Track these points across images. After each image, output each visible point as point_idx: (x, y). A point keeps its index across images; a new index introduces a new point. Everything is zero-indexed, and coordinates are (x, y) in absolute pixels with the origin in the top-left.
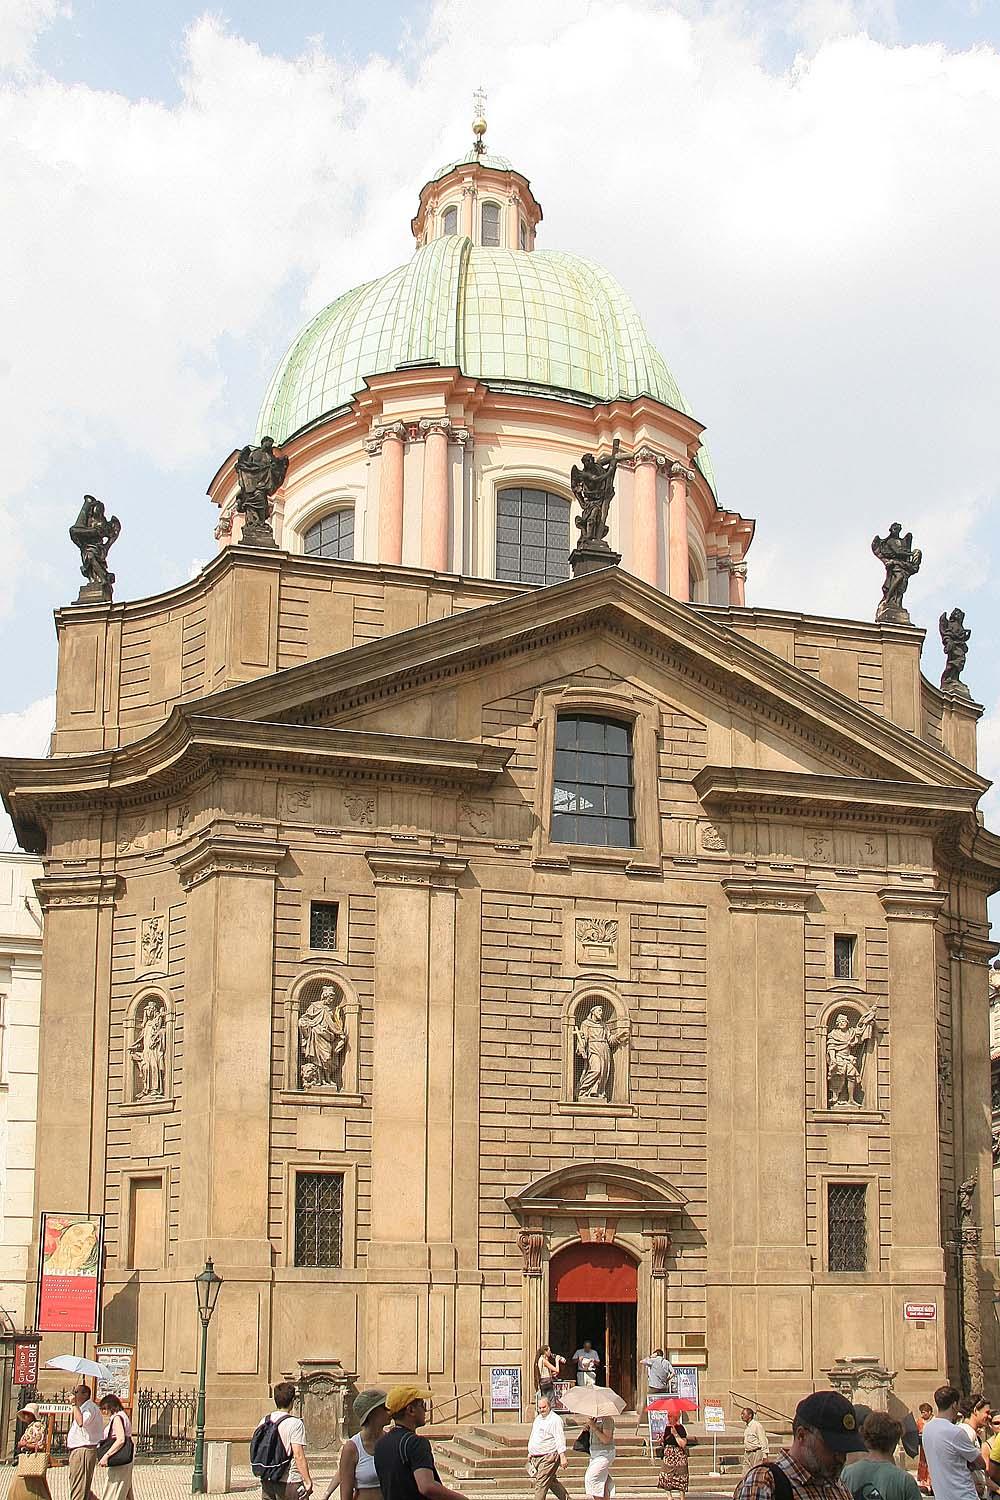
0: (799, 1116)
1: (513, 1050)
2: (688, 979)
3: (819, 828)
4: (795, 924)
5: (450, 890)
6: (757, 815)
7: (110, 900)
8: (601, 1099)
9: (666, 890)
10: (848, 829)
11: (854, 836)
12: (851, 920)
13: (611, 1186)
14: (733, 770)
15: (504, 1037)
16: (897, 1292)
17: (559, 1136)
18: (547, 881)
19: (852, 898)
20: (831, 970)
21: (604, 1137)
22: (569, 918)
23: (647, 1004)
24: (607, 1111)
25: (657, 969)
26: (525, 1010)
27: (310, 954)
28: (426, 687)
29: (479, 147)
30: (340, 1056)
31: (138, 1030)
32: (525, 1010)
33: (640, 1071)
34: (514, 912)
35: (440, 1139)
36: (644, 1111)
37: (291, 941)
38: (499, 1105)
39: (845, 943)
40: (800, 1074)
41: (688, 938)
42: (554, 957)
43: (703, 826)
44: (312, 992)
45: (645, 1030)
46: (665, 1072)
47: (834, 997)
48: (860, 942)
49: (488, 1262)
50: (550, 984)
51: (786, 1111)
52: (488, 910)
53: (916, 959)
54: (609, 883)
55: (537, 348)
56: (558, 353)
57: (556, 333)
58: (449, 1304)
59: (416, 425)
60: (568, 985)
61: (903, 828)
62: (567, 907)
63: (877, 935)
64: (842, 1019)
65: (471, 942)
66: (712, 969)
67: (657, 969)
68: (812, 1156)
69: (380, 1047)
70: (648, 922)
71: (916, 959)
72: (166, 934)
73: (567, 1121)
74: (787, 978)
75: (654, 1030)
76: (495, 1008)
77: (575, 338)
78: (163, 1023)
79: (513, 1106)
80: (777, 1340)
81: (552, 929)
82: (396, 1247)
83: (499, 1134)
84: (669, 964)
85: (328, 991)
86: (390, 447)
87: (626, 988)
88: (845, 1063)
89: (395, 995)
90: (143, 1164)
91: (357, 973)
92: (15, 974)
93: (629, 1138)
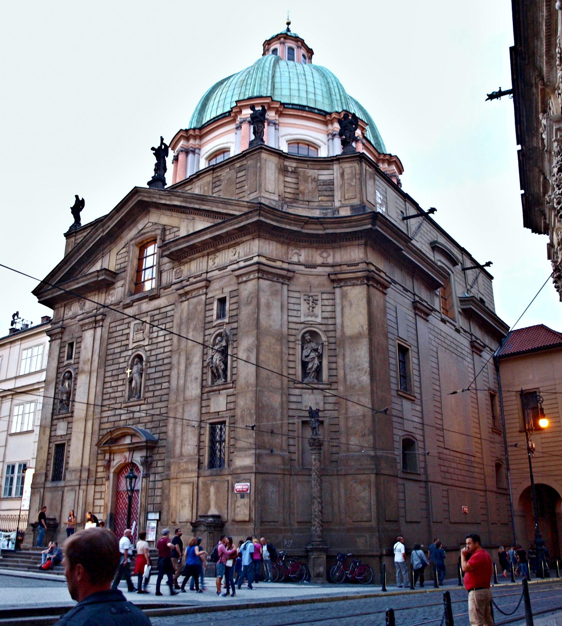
0: (199, 391)
1: (113, 384)
3: (214, 253)
4: (202, 299)
5: (100, 326)
6: (189, 257)
8: (135, 399)
10: (224, 249)
11: (227, 251)
16: (233, 477)
17: (123, 417)
19: (227, 279)
20: (215, 317)
22: (132, 326)
24: (137, 403)
25: (157, 337)
26: (117, 366)
27: (65, 363)
29: (288, 30)
32: (117, 366)
33: (149, 383)
34: (118, 328)
35: (90, 424)
36: (150, 400)
39: (222, 301)
40: (200, 371)
41: (169, 319)
43: (175, 270)
47: (216, 328)
49: (99, 475)
51: (194, 390)
52: (111, 330)
53: (249, 299)
58: (85, 493)
61: (244, 239)
62: (133, 321)
63: (235, 293)
65: (105, 344)
67: (157, 337)
68: (204, 410)
70: (156, 317)
71: (249, 299)
74: (197, 326)
80: (182, 506)
82: (74, 471)
89: (83, 372)
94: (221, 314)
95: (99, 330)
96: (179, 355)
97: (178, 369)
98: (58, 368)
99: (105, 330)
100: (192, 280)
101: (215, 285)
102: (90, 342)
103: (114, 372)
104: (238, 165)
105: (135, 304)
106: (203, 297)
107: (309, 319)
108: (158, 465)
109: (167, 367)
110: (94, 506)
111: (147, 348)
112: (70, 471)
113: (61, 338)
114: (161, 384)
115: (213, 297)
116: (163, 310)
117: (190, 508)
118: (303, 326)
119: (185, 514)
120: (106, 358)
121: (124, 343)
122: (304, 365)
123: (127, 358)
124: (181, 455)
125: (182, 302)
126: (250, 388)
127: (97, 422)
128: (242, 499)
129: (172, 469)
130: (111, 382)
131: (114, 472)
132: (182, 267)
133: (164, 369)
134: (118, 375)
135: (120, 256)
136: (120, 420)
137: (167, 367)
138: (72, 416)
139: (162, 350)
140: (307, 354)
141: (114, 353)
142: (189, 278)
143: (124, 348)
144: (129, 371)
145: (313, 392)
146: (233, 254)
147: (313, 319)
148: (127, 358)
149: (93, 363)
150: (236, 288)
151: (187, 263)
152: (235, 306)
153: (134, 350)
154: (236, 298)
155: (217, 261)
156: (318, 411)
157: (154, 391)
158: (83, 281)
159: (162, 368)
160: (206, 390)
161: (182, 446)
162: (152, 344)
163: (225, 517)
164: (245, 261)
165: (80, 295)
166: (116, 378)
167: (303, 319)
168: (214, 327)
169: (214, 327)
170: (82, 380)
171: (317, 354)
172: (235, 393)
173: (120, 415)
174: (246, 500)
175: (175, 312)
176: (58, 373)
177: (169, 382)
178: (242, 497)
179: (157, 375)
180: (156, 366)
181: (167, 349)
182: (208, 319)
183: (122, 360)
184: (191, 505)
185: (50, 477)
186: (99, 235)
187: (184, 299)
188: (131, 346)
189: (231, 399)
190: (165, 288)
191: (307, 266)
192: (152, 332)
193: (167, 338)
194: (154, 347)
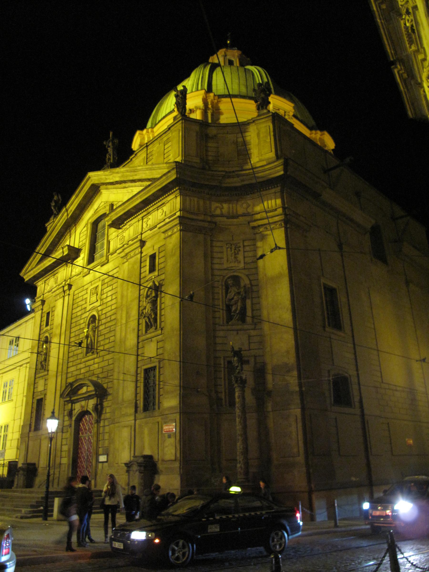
17: (83, 371)
25: (107, 297)
27: (44, 330)
28: (68, 237)
53: (174, 251)
61: (169, 198)
67: (107, 297)
70: (106, 281)
89: (55, 335)
99: (71, 297)
100: (131, 243)
101: (148, 245)
104: (165, 139)
107: (233, 265)
108: (107, 412)
109: (113, 323)
110: (61, 451)
111: (99, 308)
117: (129, 450)
118: (226, 271)
119: (125, 456)
121: (83, 306)
122: (228, 308)
123: (86, 319)
124: (123, 400)
126: (175, 332)
127: (64, 377)
128: (170, 439)
129: (116, 414)
131: (75, 421)
133: (111, 325)
136: (80, 374)
137: (113, 323)
138: (48, 374)
139: (109, 309)
140: (231, 298)
141: (77, 316)
142: (128, 241)
143: (83, 311)
144: (85, 330)
145: (238, 333)
146: (161, 214)
147: (236, 264)
148: (86, 319)
149: (62, 327)
153: (90, 312)
154: (164, 252)
156: (240, 350)
163: (156, 458)
164: (169, 217)
167: (225, 266)
169: (147, 281)
171: (240, 296)
172: (163, 338)
174: (172, 440)
175: (119, 274)
178: (169, 437)
180: (105, 323)
181: (113, 307)
183: (82, 321)
184: (129, 447)
185: (33, 428)
189: (160, 344)
190: (112, 254)
191: (228, 218)
192: (103, 294)
193: (114, 297)
194: (104, 306)
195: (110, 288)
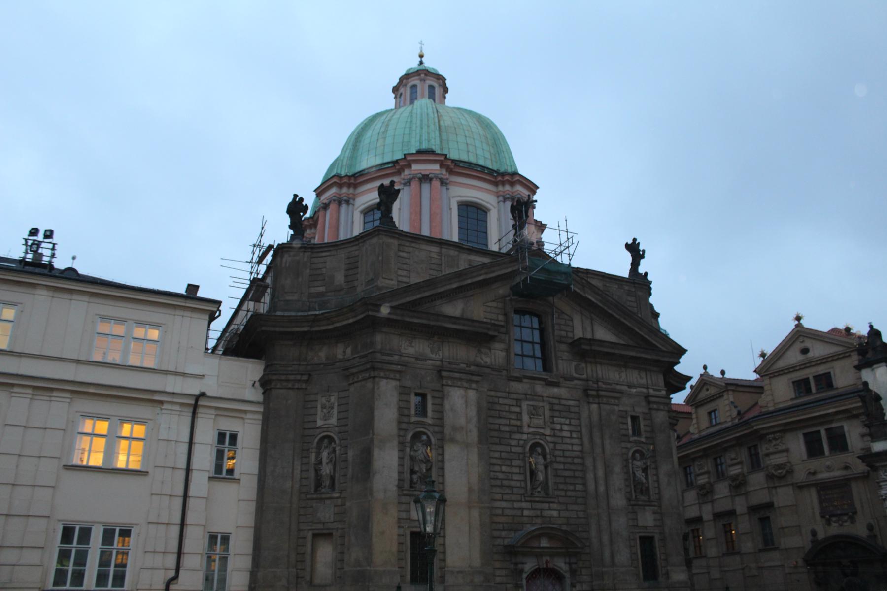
1: (504, 468)
2: (574, 435)
7: (304, 386)
8: (542, 494)
9: (560, 391)
12: (637, 409)
13: (551, 537)
14: (590, 340)
15: (499, 462)
17: (526, 513)
18: (516, 386)
20: (630, 432)
21: (545, 513)
22: (525, 405)
23: (558, 447)
25: (561, 430)
26: (508, 449)
27: (413, 419)
30: (429, 470)
31: (318, 453)
32: (508, 449)
34: (501, 401)
35: (475, 513)
36: (561, 500)
37: (406, 412)
38: (498, 497)
41: (573, 415)
42: (519, 423)
43: (574, 364)
44: (417, 436)
45: (559, 459)
46: (568, 480)
48: (641, 419)
49: (498, 579)
50: (517, 436)
51: (619, 500)
54: (539, 388)
55: (471, 148)
56: (480, 152)
57: (478, 144)
59: (428, 175)
60: (525, 437)
64: (637, 455)
66: (584, 430)
69: (448, 466)
70: (556, 407)
72: (336, 404)
73: (528, 505)
75: (562, 460)
76: (495, 447)
77: (485, 147)
78: (334, 450)
79: (505, 497)
81: (517, 409)
83: (500, 512)
84: (566, 428)
85: (424, 437)
86: (415, 184)
87: (548, 438)
88: (640, 474)
89: (453, 440)
90: (320, 526)
91: (436, 429)
92: (247, 421)
93: (555, 513)
94: (636, 431)
95: (472, 394)
96: (594, 460)
97: (595, 475)
98: (400, 422)
102: (461, 405)
103: (503, 454)
104: (627, 288)
105: (525, 380)
106: (616, 408)
112: (452, 572)
113: (399, 380)
114: (574, 484)
115: (626, 411)
116: (563, 402)
120: (490, 434)
124: (613, 564)
125: (589, 403)
130: (501, 466)
132: (584, 365)
134: (511, 460)
135: (489, 309)
139: (570, 447)
148: (522, 442)
150: (647, 411)
151: (591, 363)
152: (648, 429)
155: (623, 375)
157: (566, 491)
158: (464, 325)
159: (573, 467)
160: (632, 503)
161: (612, 556)
162: (554, 436)
164: (654, 390)
165: (438, 332)
166: (508, 463)
168: (630, 442)
170: (452, 451)
173: (522, 509)
176: (400, 429)
177: (585, 484)
179: (567, 474)
180: (564, 463)
182: (624, 432)
183: (514, 443)
185: (409, 577)
186: (481, 275)
187: (591, 400)
188: (526, 429)
190: (566, 379)
192: (553, 423)
195: (567, 422)
